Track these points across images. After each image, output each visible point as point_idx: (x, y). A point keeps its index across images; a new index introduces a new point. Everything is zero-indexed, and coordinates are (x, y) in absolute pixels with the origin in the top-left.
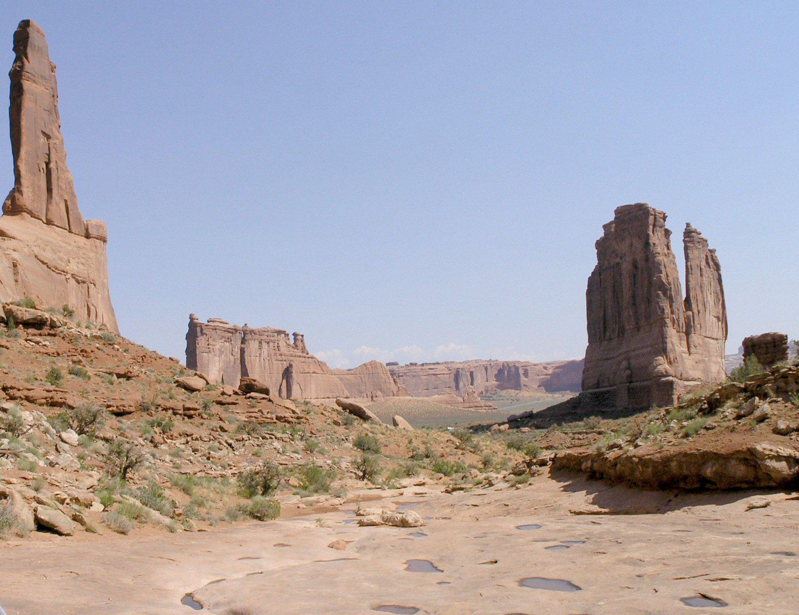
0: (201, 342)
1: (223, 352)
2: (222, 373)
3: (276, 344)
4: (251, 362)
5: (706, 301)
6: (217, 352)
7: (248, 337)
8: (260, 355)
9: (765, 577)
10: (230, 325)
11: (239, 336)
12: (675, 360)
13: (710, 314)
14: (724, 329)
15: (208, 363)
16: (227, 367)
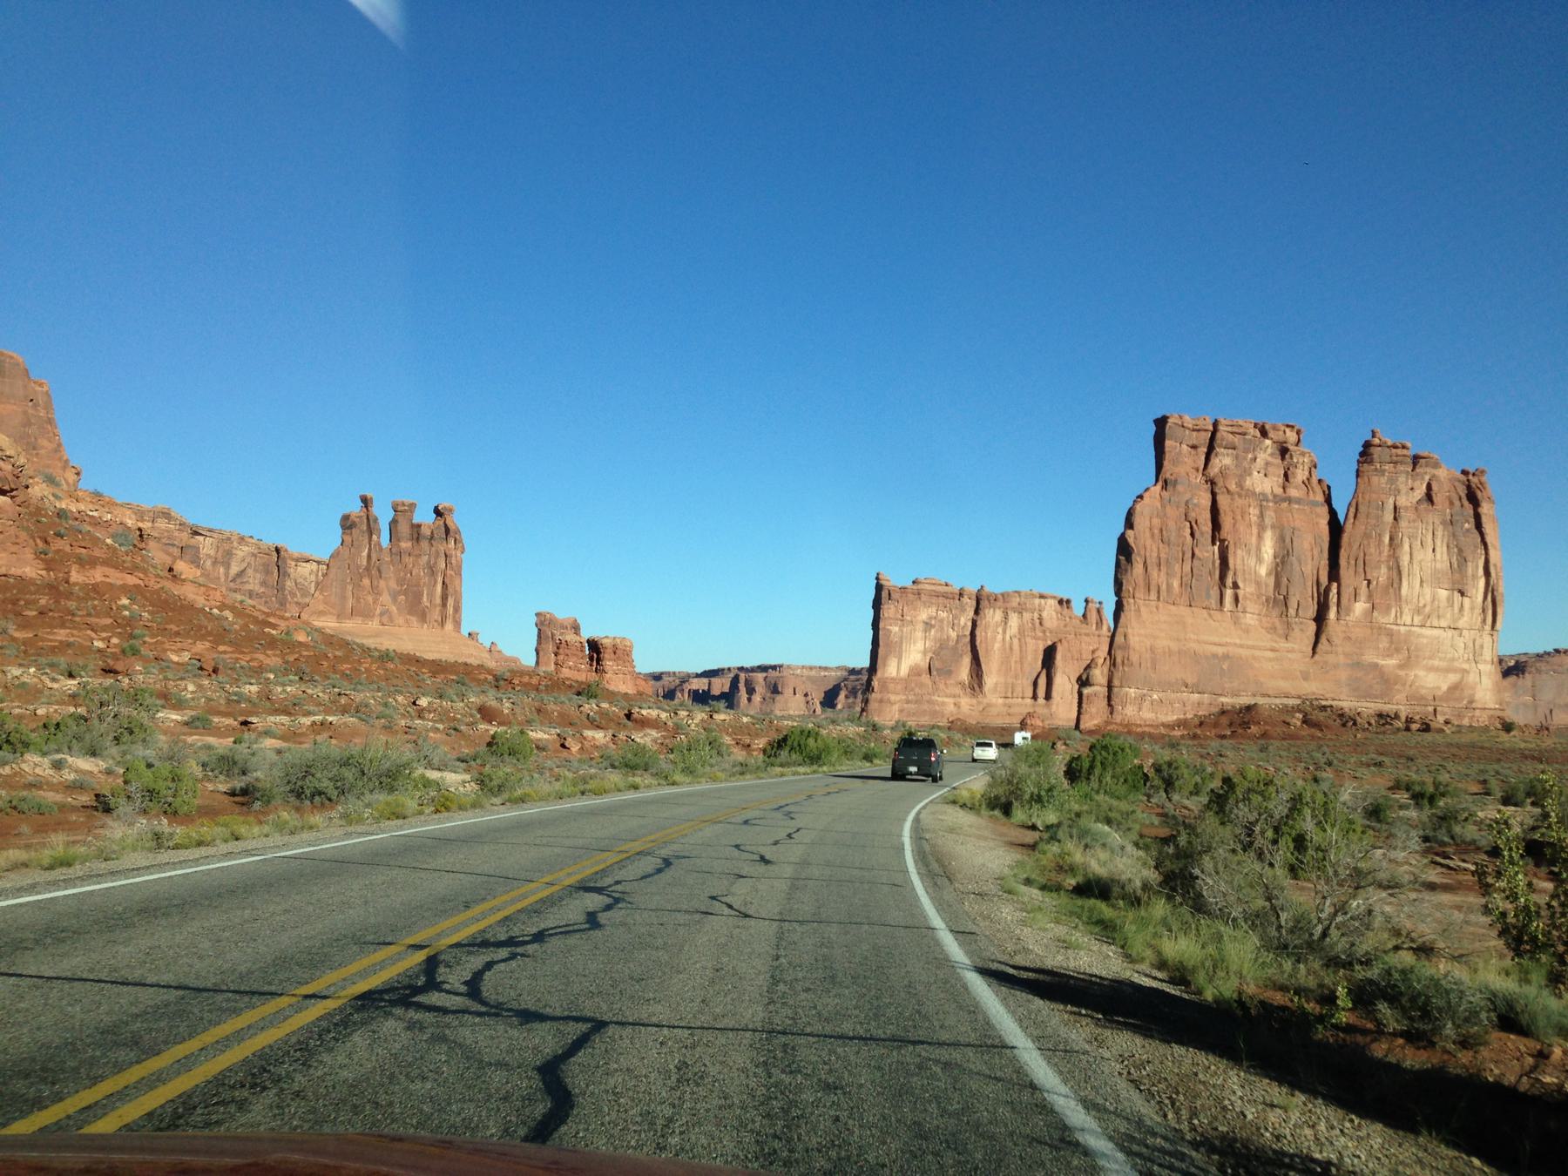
0: (888, 610)
1: (932, 626)
2: (930, 655)
3: (1036, 615)
4: (986, 643)
5: (1405, 560)
6: (920, 627)
7: (984, 603)
8: (1004, 632)
9: (1532, 1075)
10: (956, 587)
11: (970, 604)
12: (1126, 662)
13: (1421, 585)
14: (1490, 612)
15: (901, 643)
16: (941, 647)
